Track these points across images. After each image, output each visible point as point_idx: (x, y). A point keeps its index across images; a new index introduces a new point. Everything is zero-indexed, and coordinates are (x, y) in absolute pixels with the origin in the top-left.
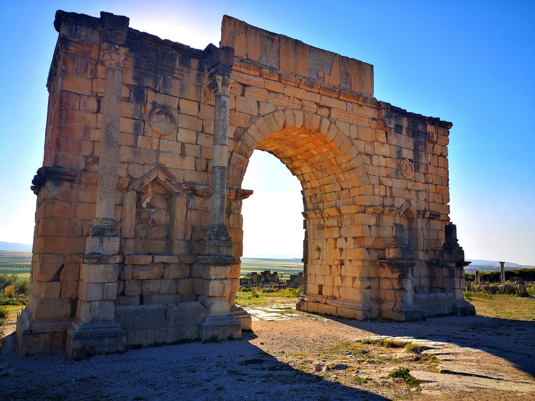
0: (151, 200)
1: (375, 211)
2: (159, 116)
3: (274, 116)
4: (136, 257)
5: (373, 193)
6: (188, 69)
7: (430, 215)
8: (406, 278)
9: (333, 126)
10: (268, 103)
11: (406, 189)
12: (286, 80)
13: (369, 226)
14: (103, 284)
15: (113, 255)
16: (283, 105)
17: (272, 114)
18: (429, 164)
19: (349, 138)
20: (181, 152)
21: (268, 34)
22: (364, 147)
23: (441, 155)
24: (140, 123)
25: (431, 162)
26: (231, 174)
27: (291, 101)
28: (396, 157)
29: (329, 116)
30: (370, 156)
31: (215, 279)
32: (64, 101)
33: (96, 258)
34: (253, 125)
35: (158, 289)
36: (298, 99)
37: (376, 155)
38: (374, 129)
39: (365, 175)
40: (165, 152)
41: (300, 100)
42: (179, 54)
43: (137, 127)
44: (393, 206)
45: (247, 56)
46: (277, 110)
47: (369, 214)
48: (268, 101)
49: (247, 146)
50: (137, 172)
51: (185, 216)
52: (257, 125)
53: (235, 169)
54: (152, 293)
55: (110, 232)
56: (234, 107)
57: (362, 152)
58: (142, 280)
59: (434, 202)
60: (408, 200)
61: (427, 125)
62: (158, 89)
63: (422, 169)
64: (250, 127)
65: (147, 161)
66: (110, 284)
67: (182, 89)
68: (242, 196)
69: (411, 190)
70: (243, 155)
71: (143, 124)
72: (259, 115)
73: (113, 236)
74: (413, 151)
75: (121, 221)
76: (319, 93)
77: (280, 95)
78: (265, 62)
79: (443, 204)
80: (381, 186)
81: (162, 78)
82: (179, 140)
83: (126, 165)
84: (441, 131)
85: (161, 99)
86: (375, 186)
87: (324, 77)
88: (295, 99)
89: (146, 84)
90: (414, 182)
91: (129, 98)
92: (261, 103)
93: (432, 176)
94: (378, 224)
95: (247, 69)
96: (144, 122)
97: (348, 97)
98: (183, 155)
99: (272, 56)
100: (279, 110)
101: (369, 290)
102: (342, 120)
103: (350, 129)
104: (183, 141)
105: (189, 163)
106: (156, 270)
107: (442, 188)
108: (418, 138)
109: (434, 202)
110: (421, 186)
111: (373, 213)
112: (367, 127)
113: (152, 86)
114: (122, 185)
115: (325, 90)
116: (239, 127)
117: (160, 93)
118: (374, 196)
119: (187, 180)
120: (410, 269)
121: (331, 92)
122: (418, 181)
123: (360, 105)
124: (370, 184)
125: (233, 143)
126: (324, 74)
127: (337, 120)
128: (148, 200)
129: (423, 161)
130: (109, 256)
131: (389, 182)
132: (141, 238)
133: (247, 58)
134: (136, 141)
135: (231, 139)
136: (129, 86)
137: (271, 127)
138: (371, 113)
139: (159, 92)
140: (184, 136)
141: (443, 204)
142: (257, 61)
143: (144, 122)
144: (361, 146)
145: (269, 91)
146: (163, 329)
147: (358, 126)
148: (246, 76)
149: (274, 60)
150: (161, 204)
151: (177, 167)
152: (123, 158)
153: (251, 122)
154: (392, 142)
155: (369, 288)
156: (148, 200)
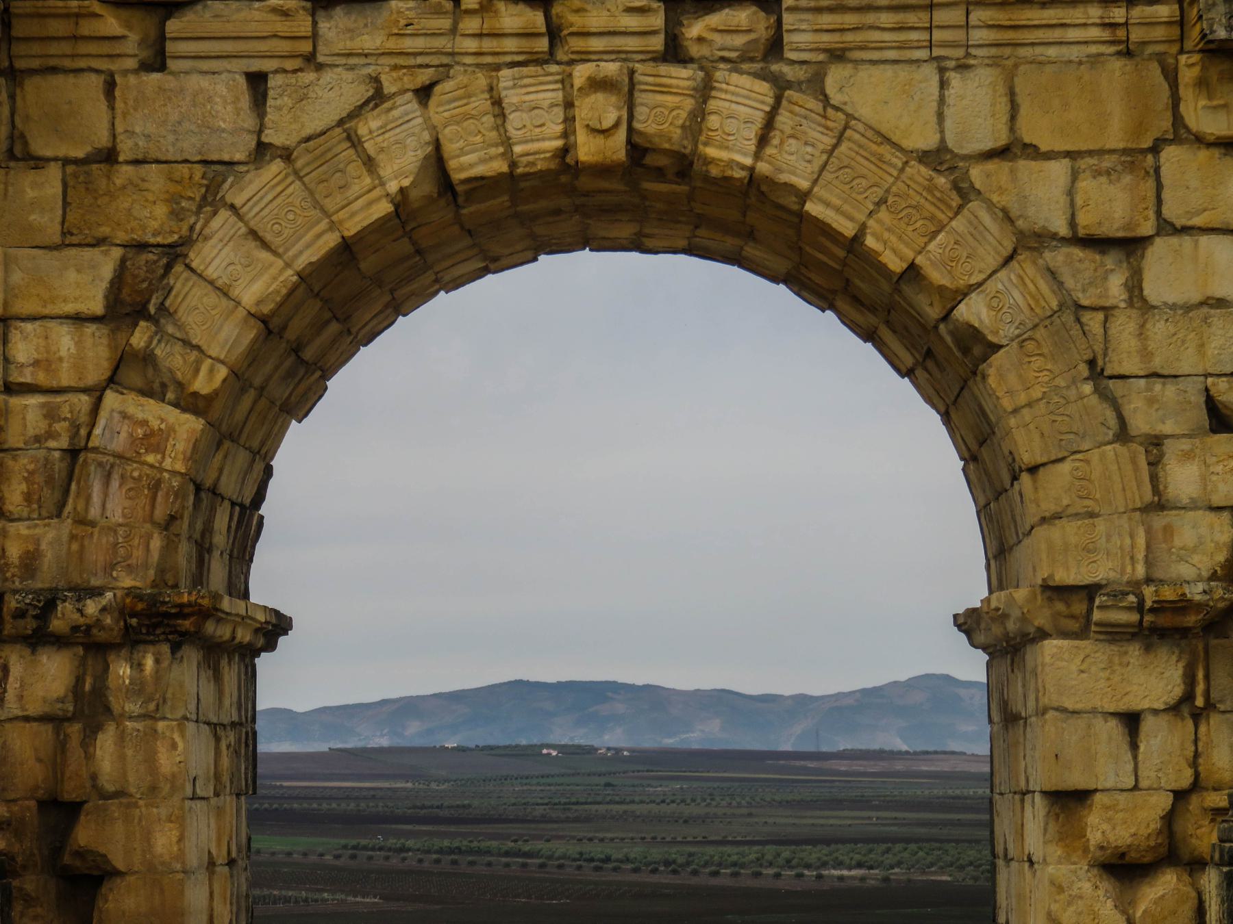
1: (1148, 618)
3: (354, 141)
5: (1148, 496)
10: (320, 67)
13: (1131, 721)
16: (420, 60)
17: (338, 130)
19: (936, 158)
22: (1063, 200)
26: (94, 512)
29: (775, 47)
34: (224, 214)
37: (1185, 230)
46: (378, 97)
47: (1114, 634)
48: (320, 59)
49: (186, 343)
52: (250, 212)
53: (115, 483)
56: (102, 139)
57: (1054, 236)
64: (207, 231)
68: (156, 626)
70: (170, 396)
72: (262, 151)
86: (1170, 447)
92: (271, 83)
94: (1200, 702)
102: (875, 55)
103: (942, 101)
112: (1095, 60)
116: (142, 247)
118: (1159, 521)
124: (1123, 434)
125: (105, 341)
127: (837, 55)
137: (330, 205)
153: (211, 199)
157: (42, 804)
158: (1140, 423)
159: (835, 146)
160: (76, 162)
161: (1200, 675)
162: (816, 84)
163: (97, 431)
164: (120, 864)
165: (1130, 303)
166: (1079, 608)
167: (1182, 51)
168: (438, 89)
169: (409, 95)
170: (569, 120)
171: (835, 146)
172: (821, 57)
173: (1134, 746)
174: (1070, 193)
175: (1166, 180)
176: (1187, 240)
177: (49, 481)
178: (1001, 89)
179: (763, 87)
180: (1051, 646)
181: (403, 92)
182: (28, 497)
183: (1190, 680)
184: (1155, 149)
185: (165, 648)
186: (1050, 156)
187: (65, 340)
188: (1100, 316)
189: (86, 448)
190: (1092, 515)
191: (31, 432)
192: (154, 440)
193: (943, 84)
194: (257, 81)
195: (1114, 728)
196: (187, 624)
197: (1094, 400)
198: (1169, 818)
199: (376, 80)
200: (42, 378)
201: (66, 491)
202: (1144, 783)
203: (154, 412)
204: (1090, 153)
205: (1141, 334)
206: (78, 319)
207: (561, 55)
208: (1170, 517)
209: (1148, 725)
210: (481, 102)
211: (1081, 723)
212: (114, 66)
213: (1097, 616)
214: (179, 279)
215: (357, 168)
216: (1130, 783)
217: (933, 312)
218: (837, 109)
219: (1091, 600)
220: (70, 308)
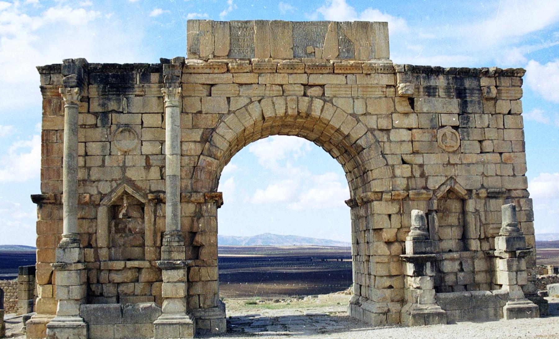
0: (126, 211)
2: (123, 134)
3: (247, 110)
4: (110, 263)
6: (149, 85)
7: (488, 193)
8: (423, 275)
9: (328, 105)
10: (240, 96)
11: (447, 164)
12: (259, 69)
14: (68, 286)
15: (74, 263)
18: (488, 127)
19: (353, 115)
20: (146, 163)
21: (240, 24)
22: (375, 122)
23: (509, 113)
24: (106, 145)
25: (491, 123)
26: (199, 178)
27: (268, 89)
28: (429, 127)
29: (324, 94)
30: (388, 131)
31: (168, 282)
32: (45, 138)
33: (60, 266)
35: (131, 291)
36: (278, 85)
37: (396, 128)
38: (392, 98)
39: (378, 155)
40: (130, 167)
41: (282, 85)
42: (139, 73)
43: (104, 148)
44: (426, 188)
45: (213, 53)
46: (251, 102)
47: (387, 201)
49: (216, 146)
50: (105, 188)
51: (153, 224)
52: (227, 123)
54: (126, 294)
55: (71, 244)
56: (200, 110)
58: (118, 284)
59: (497, 175)
60: (451, 178)
61: (480, 78)
62: (121, 110)
63: (476, 135)
65: (114, 177)
66: (73, 287)
67: (144, 105)
69: (457, 164)
71: (108, 144)
72: (229, 112)
73: (73, 248)
74: (459, 114)
75: (96, 233)
76: (305, 73)
77: (254, 85)
78: (238, 53)
79: (514, 175)
80: (405, 166)
81: (125, 99)
82: (143, 153)
83: (96, 183)
84: (505, 82)
85: (124, 119)
86: (395, 166)
87: (315, 52)
88: (274, 86)
89: (110, 109)
90: (462, 154)
91: (96, 124)
92: (231, 99)
93: (493, 142)
94: (402, 212)
95: (210, 68)
96: (110, 142)
97: (347, 69)
98: (148, 166)
99: (246, 45)
100: (253, 102)
101: (389, 291)
103: (353, 104)
104: (147, 154)
105: (154, 173)
106: (130, 275)
107: (512, 156)
108: (465, 97)
109: (497, 175)
110: (473, 158)
111: (392, 200)
112: (380, 98)
113: (116, 109)
114: (94, 201)
115: (313, 69)
116: (207, 129)
117: (123, 113)
118: (394, 180)
119: (153, 189)
120: (428, 264)
121: (321, 68)
122: (467, 151)
123: (367, 74)
126: (314, 49)
127: (335, 97)
128: (124, 211)
129: (478, 124)
130: (71, 264)
131: (418, 160)
132: (120, 246)
133: (214, 56)
134: (103, 161)
135: (199, 142)
136: (96, 114)
138: (385, 80)
139: (122, 112)
140: (147, 148)
141: (514, 174)
142: (228, 56)
143: (110, 142)
144: (372, 122)
145: (241, 85)
146: (120, 325)
147: (365, 99)
148: (211, 76)
149: (249, 49)
150: (135, 214)
151: (142, 179)
152: (93, 178)
154: (422, 109)
155: (391, 287)
156: (124, 211)
157: (189, 232)
158: (390, 162)
159: (335, 112)
160: (195, 113)
161: (402, 207)
162: (331, 101)
163: (199, 163)
164: (204, 244)
165: (388, 141)
166: (380, 195)
167: (395, 97)
168: (262, 100)
169: (257, 102)
170: (287, 107)
171: (335, 112)
172: (332, 96)
173: (390, 220)
174: (377, 121)
175: (393, 119)
176: (397, 130)
177: (190, 172)
178: (364, 103)
179: (321, 101)
180: (375, 203)
181: (256, 101)
182: (186, 175)
183: (400, 209)
184: (391, 114)
185: (213, 203)
186: (373, 115)
187: (192, 145)
188: (383, 143)
189: (197, 166)
190: (382, 179)
191: (186, 163)
192: (210, 164)
193: (354, 102)
194: (228, 98)
195: (387, 217)
196: (217, 199)
197: (382, 158)
198: (397, 233)
199: (251, 99)
200: (189, 153)
201: (193, 174)
202: (392, 227)
203: (209, 159)
204: (380, 114)
205: (390, 146)
206: (195, 142)
207: (284, 95)
208: (396, 179)
209: (393, 216)
210: (270, 103)
211: (380, 216)
212: (202, 95)
213: (384, 197)
214: (214, 134)
215: (247, 115)
216: (390, 227)
217: (354, 142)
218: (335, 106)
219: (382, 195)
220: (193, 140)
